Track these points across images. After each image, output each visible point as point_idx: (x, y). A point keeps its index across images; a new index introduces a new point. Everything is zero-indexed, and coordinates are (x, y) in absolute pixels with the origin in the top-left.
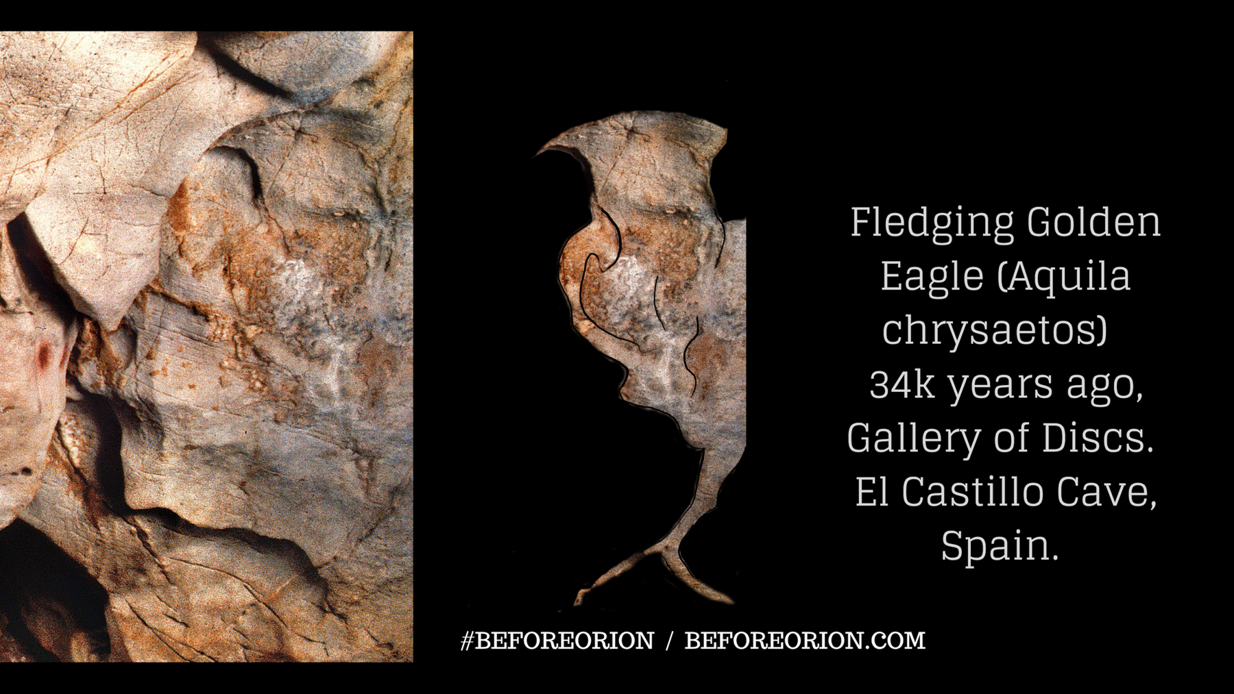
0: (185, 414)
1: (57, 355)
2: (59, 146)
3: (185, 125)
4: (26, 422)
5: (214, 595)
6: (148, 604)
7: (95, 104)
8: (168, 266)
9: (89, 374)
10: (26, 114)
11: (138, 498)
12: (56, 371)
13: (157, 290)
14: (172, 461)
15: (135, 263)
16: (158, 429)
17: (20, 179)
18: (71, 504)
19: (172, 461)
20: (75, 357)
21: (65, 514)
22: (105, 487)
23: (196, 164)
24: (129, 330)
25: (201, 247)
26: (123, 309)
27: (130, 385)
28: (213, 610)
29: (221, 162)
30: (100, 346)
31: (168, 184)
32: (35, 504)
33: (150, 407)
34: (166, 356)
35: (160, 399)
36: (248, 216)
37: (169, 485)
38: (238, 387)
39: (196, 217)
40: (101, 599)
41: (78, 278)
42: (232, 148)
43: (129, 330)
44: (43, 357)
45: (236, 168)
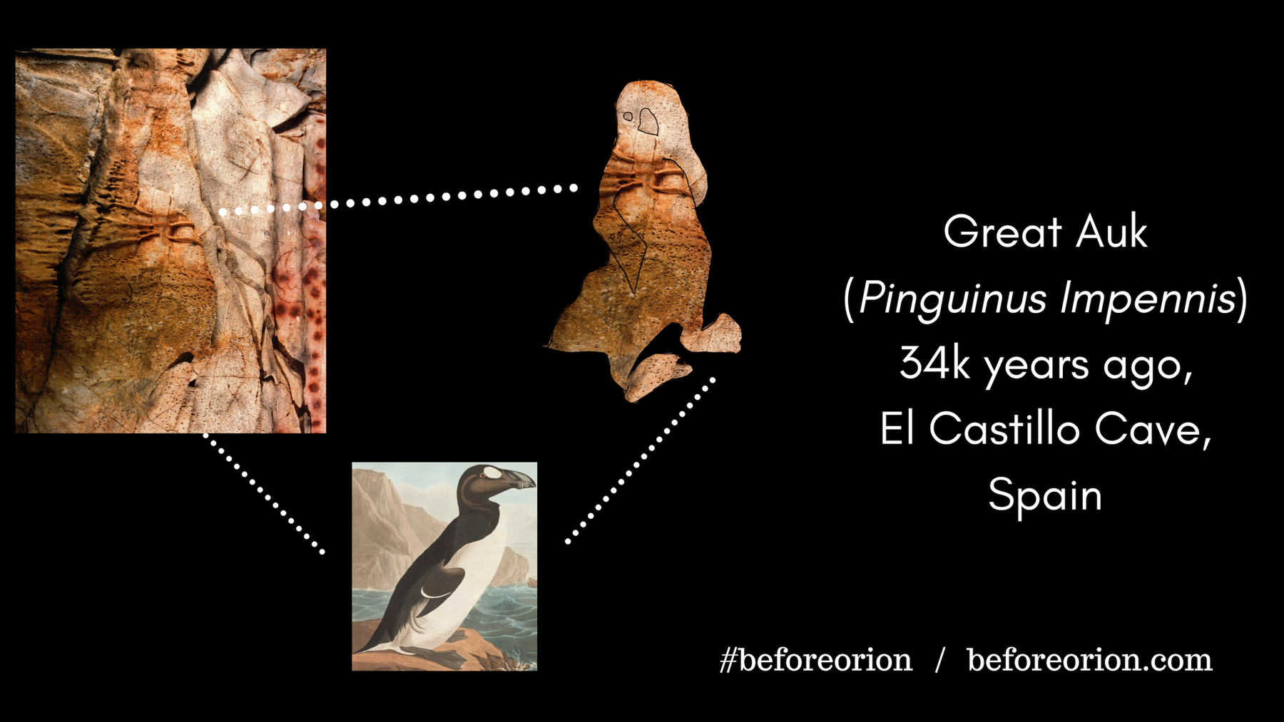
2: (250, 116)
3: (243, 75)
7: (236, 104)
8: (290, 80)
10: (239, 127)
13: (298, 84)
15: (289, 91)
17: (261, 129)
24: (311, 93)
25: (284, 69)
30: (317, 103)
31: (263, 80)
39: (274, 71)
41: (294, 110)
43: (311, 93)
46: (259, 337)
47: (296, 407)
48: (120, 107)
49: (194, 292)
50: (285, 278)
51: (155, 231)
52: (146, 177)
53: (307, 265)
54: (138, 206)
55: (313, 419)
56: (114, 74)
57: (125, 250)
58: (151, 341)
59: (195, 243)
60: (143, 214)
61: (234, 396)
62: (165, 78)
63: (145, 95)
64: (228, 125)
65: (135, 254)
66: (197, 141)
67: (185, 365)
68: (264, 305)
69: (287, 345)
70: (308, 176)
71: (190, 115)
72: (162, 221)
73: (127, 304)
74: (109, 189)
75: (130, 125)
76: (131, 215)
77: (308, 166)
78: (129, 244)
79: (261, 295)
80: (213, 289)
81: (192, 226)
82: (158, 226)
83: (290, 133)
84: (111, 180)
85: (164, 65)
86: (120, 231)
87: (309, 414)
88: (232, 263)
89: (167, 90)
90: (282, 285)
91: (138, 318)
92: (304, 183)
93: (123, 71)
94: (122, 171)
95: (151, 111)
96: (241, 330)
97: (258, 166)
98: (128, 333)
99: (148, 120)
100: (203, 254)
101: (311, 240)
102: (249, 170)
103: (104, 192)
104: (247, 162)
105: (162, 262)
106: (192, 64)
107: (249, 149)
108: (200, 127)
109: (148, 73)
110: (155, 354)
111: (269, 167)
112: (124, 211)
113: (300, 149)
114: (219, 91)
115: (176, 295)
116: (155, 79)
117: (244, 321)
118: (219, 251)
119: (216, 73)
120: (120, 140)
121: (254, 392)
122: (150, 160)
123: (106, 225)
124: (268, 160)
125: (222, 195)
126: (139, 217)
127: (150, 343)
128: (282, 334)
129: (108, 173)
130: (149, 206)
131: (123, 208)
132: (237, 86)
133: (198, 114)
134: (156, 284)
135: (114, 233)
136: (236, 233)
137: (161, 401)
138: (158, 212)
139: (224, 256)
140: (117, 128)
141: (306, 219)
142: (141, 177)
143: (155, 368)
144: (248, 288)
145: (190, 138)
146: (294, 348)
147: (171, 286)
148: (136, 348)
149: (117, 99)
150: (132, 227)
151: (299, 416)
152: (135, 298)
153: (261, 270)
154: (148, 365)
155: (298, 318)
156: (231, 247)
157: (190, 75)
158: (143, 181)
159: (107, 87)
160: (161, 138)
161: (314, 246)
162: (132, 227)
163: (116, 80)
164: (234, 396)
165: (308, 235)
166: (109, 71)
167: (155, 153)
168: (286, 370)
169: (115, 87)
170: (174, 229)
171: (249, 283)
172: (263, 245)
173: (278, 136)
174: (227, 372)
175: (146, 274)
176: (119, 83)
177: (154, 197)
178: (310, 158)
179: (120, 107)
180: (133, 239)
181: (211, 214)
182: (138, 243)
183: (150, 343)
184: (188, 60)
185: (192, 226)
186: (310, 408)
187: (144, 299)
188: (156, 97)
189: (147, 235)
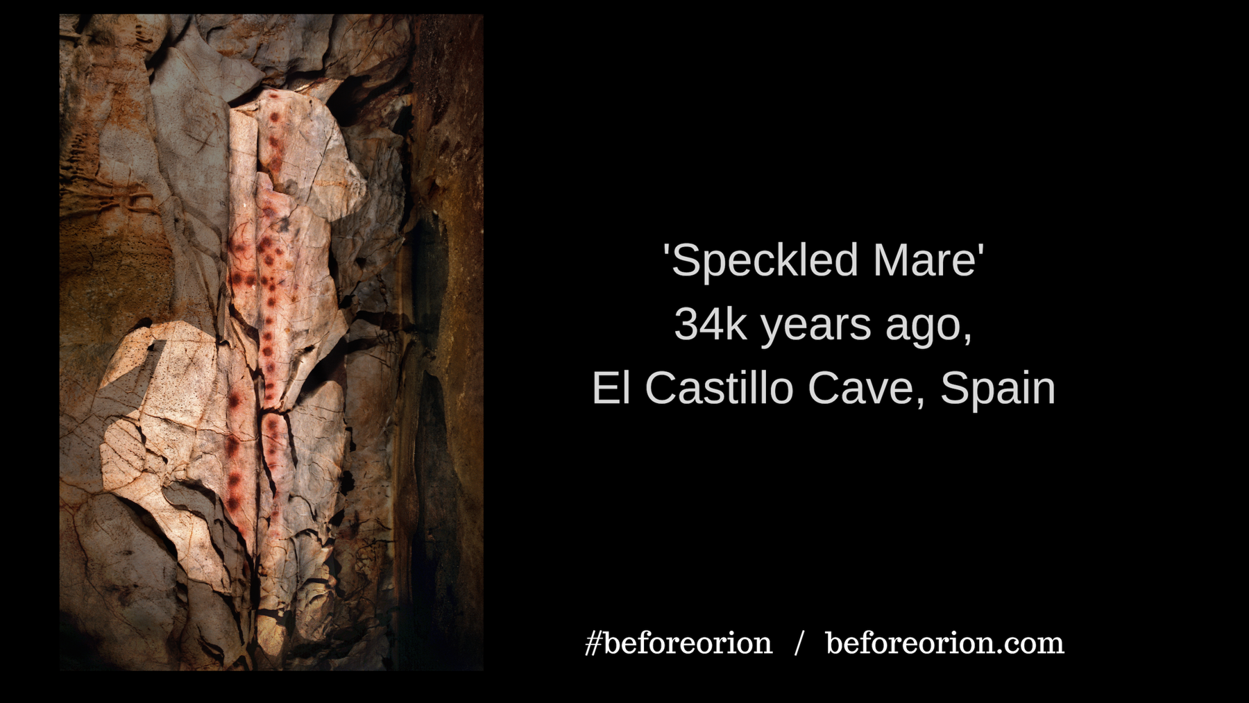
0: (292, 51)
1: (273, 92)
2: (206, 91)
3: (199, 51)
4: (295, 102)
5: (350, 42)
6: (353, 63)
7: (193, 80)
8: (245, 56)
9: (279, 82)
10: (196, 102)
11: (319, 66)
12: (279, 92)
13: (252, 60)
14: (307, 55)
16: (297, 60)
17: (217, 104)
18: (321, 88)
19: (307, 55)
20: (275, 87)
21: (325, 89)
22: (315, 77)
23: (212, 47)
24: (265, 69)
25: (239, 46)
26: (259, 71)
27: (283, 69)
28: (355, 42)
29: (211, 39)
30: (271, 78)
32: (321, 99)
33: (290, 62)
34: (274, 57)
35: (288, 59)
36: (229, 31)
37: (315, 56)
38: (284, 34)
39: (229, 48)
40: (351, 78)
41: (249, 85)
42: (207, 36)
43: (265, 69)
44: (274, 96)
45: (213, 34)
46: (215, 303)
47: (251, 370)
48: (82, 82)
49: (152, 260)
50: (241, 248)
51: (115, 202)
52: (107, 149)
53: (262, 234)
54: (98, 178)
55: (267, 382)
56: (75, 51)
57: (86, 220)
58: (112, 307)
59: (153, 213)
60: (103, 185)
61: (191, 359)
62: (125, 55)
63: (105, 70)
64: (186, 99)
65: (96, 223)
66: (156, 115)
67: (144, 330)
68: (219, 273)
69: (243, 313)
70: (262, 149)
71: (149, 90)
72: (121, 191)
73: (88, 271)
74: (71, 161)
75: (91, 99)
76: (92, 186)
77: (262, 139)
78: (90, 213)
79: (217, 263)
80: (171, 257)
81: (151, 197)
82: (118, 196)
83: (245, 108)
84: (73, 152)
85: (124, 42)
86: (82, 201)
87: (263, 377)
88: (189, 232)
89: (127, 66)
90: (239, 255)
91: (99, 285)
92: (258, 155)
93: (84, 48)
94: (83, 144)
95: (111, 87)
96: (198, 297)
97: (214, 139)
98: (90, 299)
99: (109, 95)
100: (162, 224)
101: (265, 210)
102: (205, 143)
103: (66, 164)
104: (204, 136)
105: (122, 231)
106: (150, 41)
107: (205, 123)
108: (158, 101)
109: (108, 50)
110: (115, 319)
111: (225, 140)
112: (85, 182)
113: (255, 123)
114: (177, 67)
115: (135, 263)
116: (115, 55)
117: (201, 288)
118: (176, 220)
119: (173, 50)
120: (81, 114)
121: (211, 356)
122: (110, 133)
123: (68, 196)
124: (223, 133)
125: (180, 166)
126: (100, 188)
127: (110, 309)
128: (239, 302)
129: (70, 146)
130: (110, 177)
131: (84, 179)
132: (194, 62)
133: (156, 89)
134: (116, 252)
135: (76, 204)
136: (193, 203)
137: (121, 364)
138: (118, 183)
139: (181, 225)
140: (78, 102)
141: (260, 190)
142: (102, 149)
143: (115, 332)
144: (204, 256)
145: (148, 113)
146: (250, 315)
147: (130, 254)
148: (97, 314)
149: (78, 75)
150: (93, 198)
151: (254, 378)
152: (96, 266)
153: (217, 239)
154: (108, 330)
155: (254, 287)
156: (189, 217)
157: (149, 52)
158: (104, 153)
159: (69, 64)
160: (121, 113)
161: (268, 216)
162: (93, 198)
163: (78, 56)
164: (191, 359)
165: (262, 205)
166: (70, 47)
167: (115, 126)
168: (242, 336)
169: (77, 63)
170: (134, 200)
171: (206, 251)
172: (219, 215)
173: (233, 111)
174: (185, 336)
175: (107, 243)
176: (81, 59)
177: (114, 169)
178: (264, 132)
179: (82, 82)
180: (94, 209)
181: (169, 185)
182: (99, 213)
183: (110, 309)
184: (147, 38)
185: (151, 197)
186: (264, 371)
187: (104, 267)
188: (116, 72)
189: (107, 205)
